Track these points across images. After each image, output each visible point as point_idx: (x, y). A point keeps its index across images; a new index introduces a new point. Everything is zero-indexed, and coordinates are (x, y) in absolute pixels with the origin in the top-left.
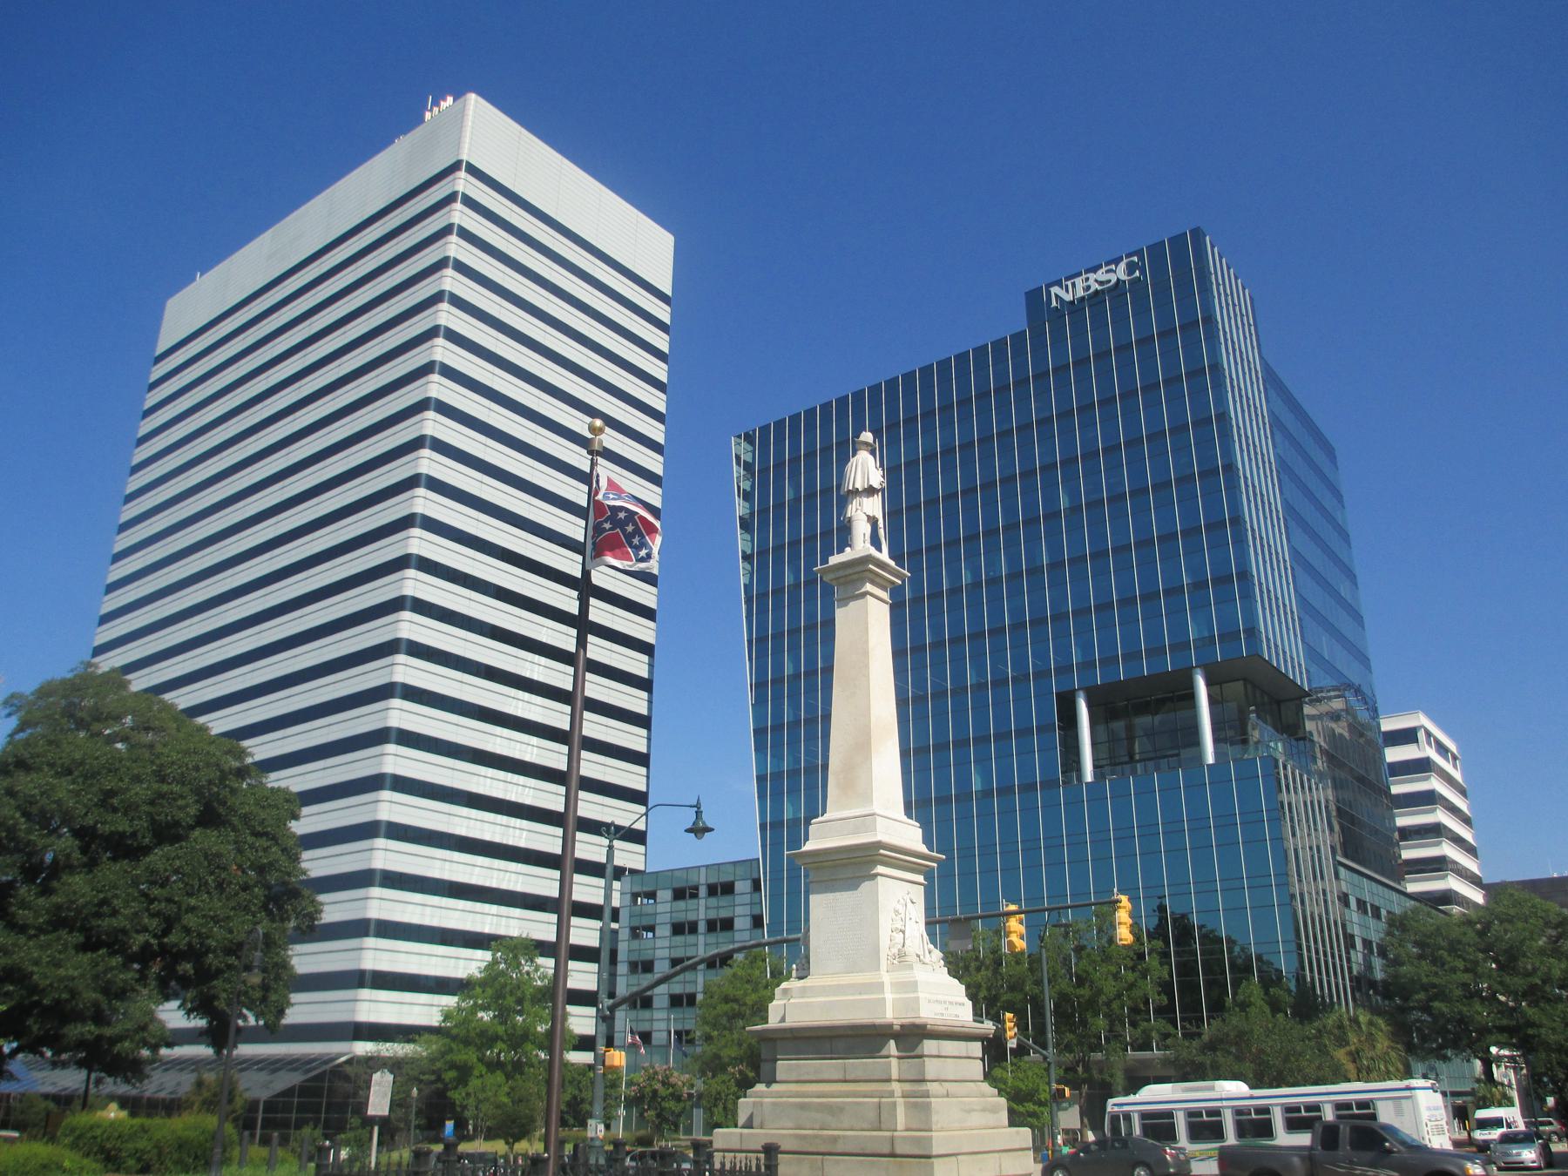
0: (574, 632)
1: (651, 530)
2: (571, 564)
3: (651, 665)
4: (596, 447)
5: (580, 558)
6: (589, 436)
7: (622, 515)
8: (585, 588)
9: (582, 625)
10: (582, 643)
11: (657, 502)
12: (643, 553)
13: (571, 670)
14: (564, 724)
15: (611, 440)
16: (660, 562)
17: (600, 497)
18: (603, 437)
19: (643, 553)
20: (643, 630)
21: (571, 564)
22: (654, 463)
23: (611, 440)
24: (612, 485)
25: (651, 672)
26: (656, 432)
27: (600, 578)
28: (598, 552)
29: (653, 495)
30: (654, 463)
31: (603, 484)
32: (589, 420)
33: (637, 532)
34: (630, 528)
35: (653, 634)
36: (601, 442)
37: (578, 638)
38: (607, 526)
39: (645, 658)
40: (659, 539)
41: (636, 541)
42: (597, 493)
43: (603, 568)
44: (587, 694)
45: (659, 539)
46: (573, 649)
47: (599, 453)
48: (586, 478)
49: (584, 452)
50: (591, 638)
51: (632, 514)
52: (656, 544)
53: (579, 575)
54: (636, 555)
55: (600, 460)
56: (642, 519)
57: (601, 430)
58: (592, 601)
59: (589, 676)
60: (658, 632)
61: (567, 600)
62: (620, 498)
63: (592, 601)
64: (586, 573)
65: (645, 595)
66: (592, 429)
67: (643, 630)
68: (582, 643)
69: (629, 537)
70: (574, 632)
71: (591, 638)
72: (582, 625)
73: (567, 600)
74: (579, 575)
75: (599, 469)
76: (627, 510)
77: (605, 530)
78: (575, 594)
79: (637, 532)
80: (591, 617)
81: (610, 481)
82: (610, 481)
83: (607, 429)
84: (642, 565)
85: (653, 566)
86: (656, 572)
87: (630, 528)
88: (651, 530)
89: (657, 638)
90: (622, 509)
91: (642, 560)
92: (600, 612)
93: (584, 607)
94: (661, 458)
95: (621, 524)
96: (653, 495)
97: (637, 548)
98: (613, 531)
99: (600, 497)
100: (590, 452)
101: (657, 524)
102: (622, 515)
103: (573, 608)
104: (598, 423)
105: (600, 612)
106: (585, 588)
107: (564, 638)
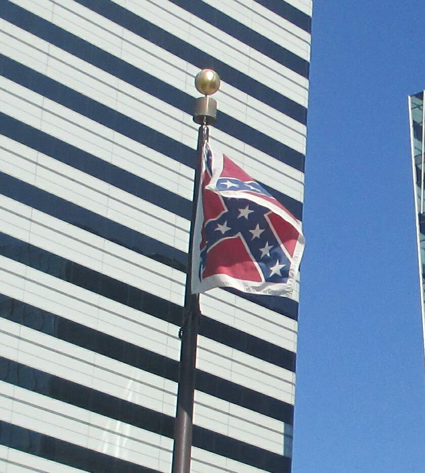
0: (174, 386)
1: (289, 234)
2: (169, 285)
3: (288, 437)
4: (207, 111)
5: (182, 277)
6: (197, 94)
7: (245, 213)
8: (190, 321)
9: (187, 376)
10: (185, 403)
11: (296, 193)
12: (276, 269)
13: (169, 443)
14: (169, 408)
15: (230, 101)
16: (302, 283)
17: (212, 186)
18: (216, 96)
19: (276, 269)
20: (276, 383)
21: (169, 285)
22: (293, 134)
23: (230, 101)
24: (230, 168)
25: (288, 445)
26: (295, 88)
27: (214, 305)
28: (210, 268)
29: (291, 183)
30: (293, 134)
31: (217, 165)
32: (195, 70)
33: (267, 237)
34: (257, 232)
35: (291, 389)
36: (213, 103)
37: (179, 396)
38: (223, 228)
39: (280, 425)
40: (299, 249)
41: (266, 251)
42: (207, 180)
43: (216, 292)
44: (196, 421)
45: (299, 249)
46: (172, 412)
47: (210, 121)
48: (190, 157)
49: (189, 119)
50: (198, 396)
51: (259, 211)
52: (296, 254)
53: (181, 302)
54: (266, 272)
55: (213, 131)
56: (275, 218)
57: (214, 87)
58: (201, 340)
59: (196, 452)
60: (299, 387)
61: (164, 340)
62: (242, 187)
63: (201, 340)
64: (192, 299)
65: (280, 331)
66: (201, 84)
67: (276, 383)
68: (185, 403)
69: (256, 246)
70: (174, 386)
71: (198, 396)
72: (187, 376)
73: (164, 340)
74: (181, 302)
75: (211, 144)
76: (252, 205)
77: (219, 235)
78: (175, 330)
79: (267, 237)
80: (200, 365)
81: (226, 160)
82: (226, 160)
83: (223, 85)
84: (275, 287)
85: (292, 289)
86: (295, 296)
87: (257, 232)
88: (289, 234)
89: (297, 395)
90: (244, 203)
91: (275, 279)
92: (212, 357)
93: (189, 349)
94: (302, 128)
95: (244, 226)
96: (291, 183)
97: (268, 262)
98: (231, 236)
99: (212, 186)
100: (198, 119)
101: (298, 226)
102: (245, 213)
103: (172, 350)
104: (210, 75)
105: (212, 357)
106: (190, 321)
107: (160, 395)
